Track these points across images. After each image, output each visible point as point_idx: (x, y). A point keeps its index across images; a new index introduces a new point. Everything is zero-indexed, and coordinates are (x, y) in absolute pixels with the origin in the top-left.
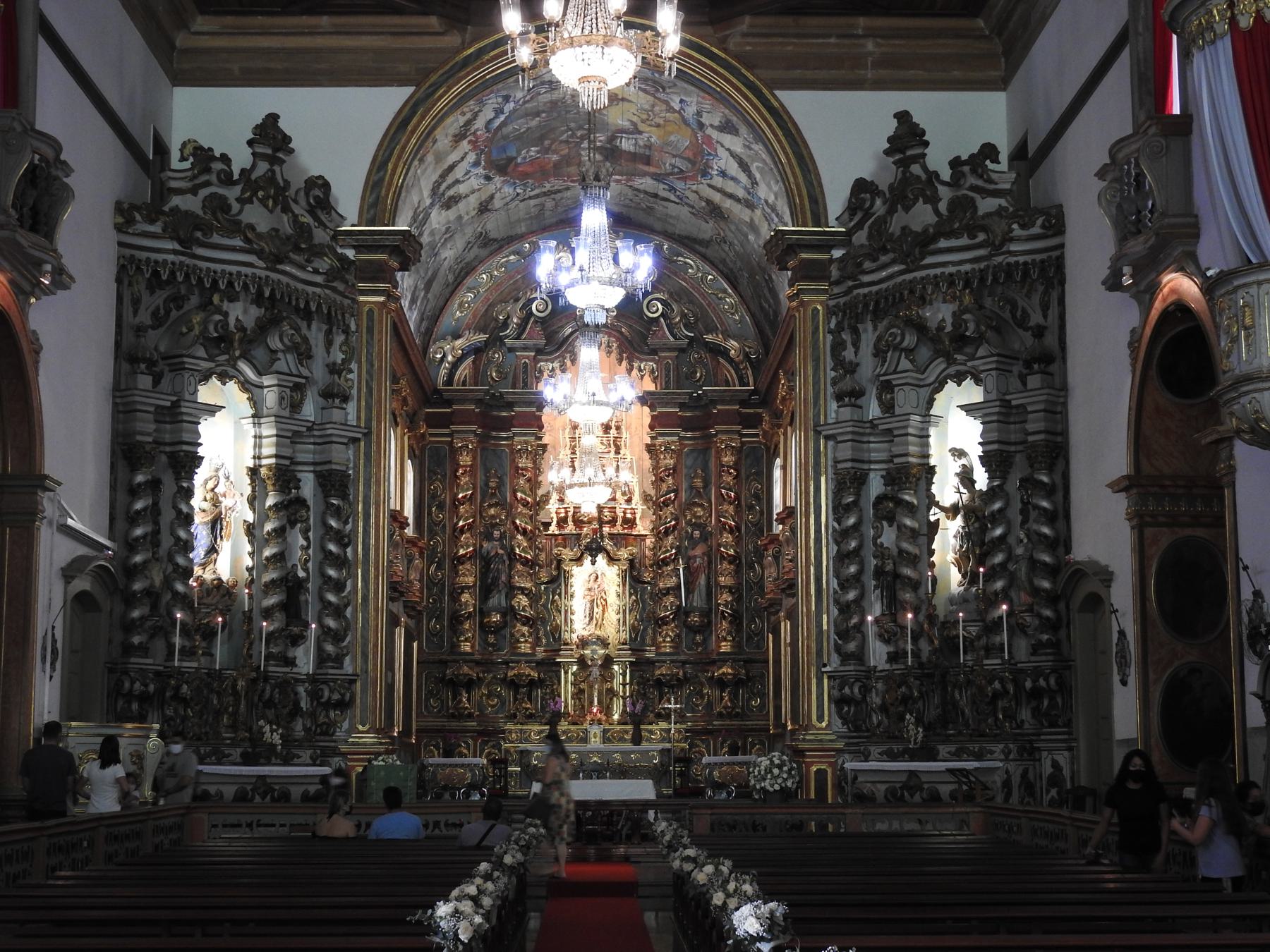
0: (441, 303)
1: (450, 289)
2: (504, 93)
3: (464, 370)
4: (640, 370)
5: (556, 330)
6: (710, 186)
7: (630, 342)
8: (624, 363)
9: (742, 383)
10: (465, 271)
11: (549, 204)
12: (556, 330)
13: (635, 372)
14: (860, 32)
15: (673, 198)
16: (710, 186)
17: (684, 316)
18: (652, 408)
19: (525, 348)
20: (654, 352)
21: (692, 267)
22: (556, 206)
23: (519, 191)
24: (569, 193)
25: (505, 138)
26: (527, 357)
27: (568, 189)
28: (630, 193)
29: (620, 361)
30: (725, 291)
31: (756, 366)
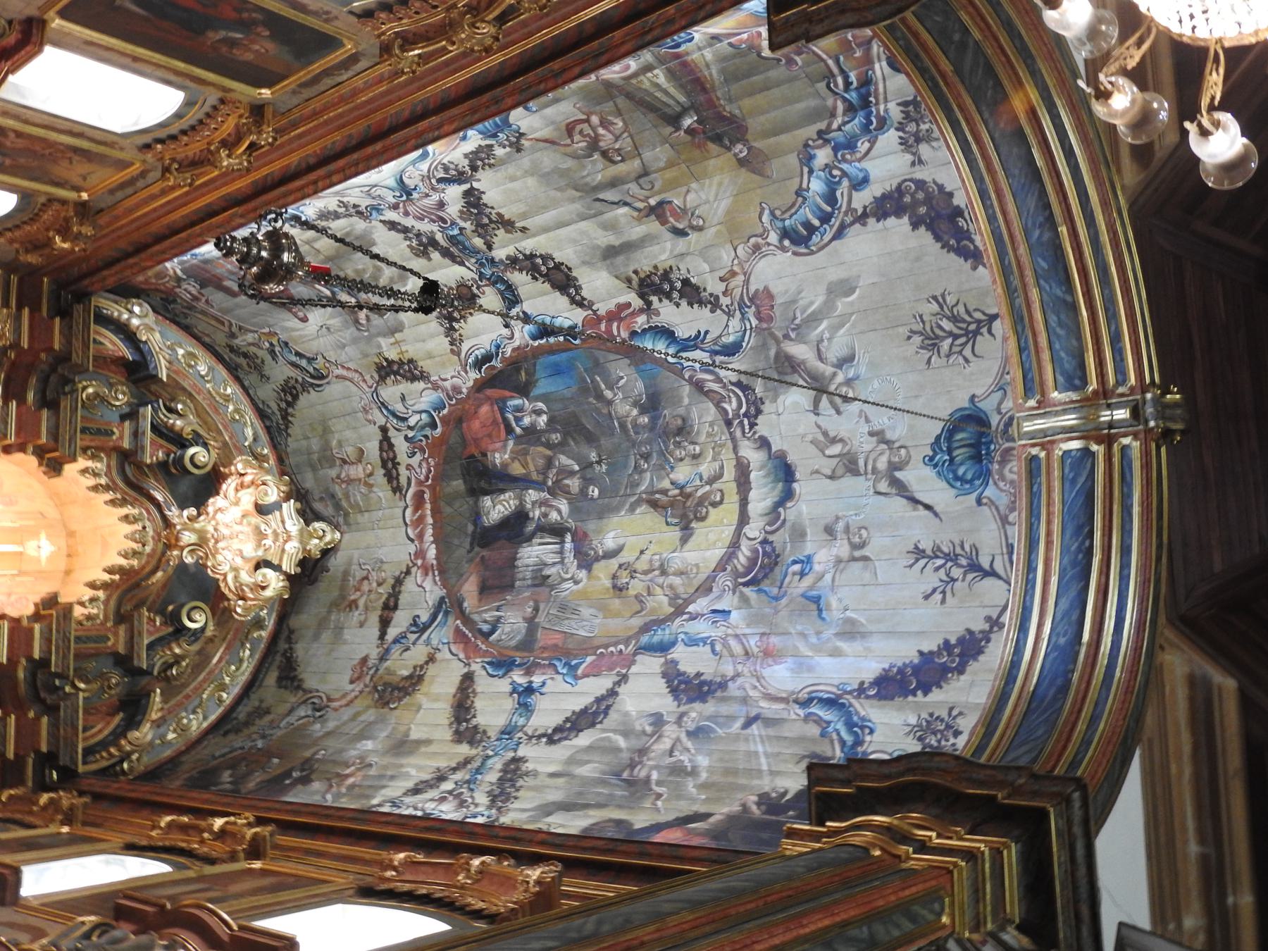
0: (201, 326)
1: (220, 339)
2: (750, 341)
3: (113, 344)
4: (92, 600)
5: (170, 476)
6: (468, 678)
7: (137, 585)
8: (106, 577)
9: (88, 751)
10: (238, 363)
11: (357, 471)
12: (170, 476)
13: (88, 594)
14: (1230, 900)
15: (392, 633)
16: (468, 678)
17: (178, 660)
18: (36, 617)
19: (136, 434)
20: (122, 617)
21: (237, 669)
22: (350, 481)
23: (412, 422)
24: (382, 491)
25: (597, 367)
26: (121, 437)
27: (397, 489)
28: (390, 573)
29: (110, 571)
30: (205, 718)
31: (109, 772)
